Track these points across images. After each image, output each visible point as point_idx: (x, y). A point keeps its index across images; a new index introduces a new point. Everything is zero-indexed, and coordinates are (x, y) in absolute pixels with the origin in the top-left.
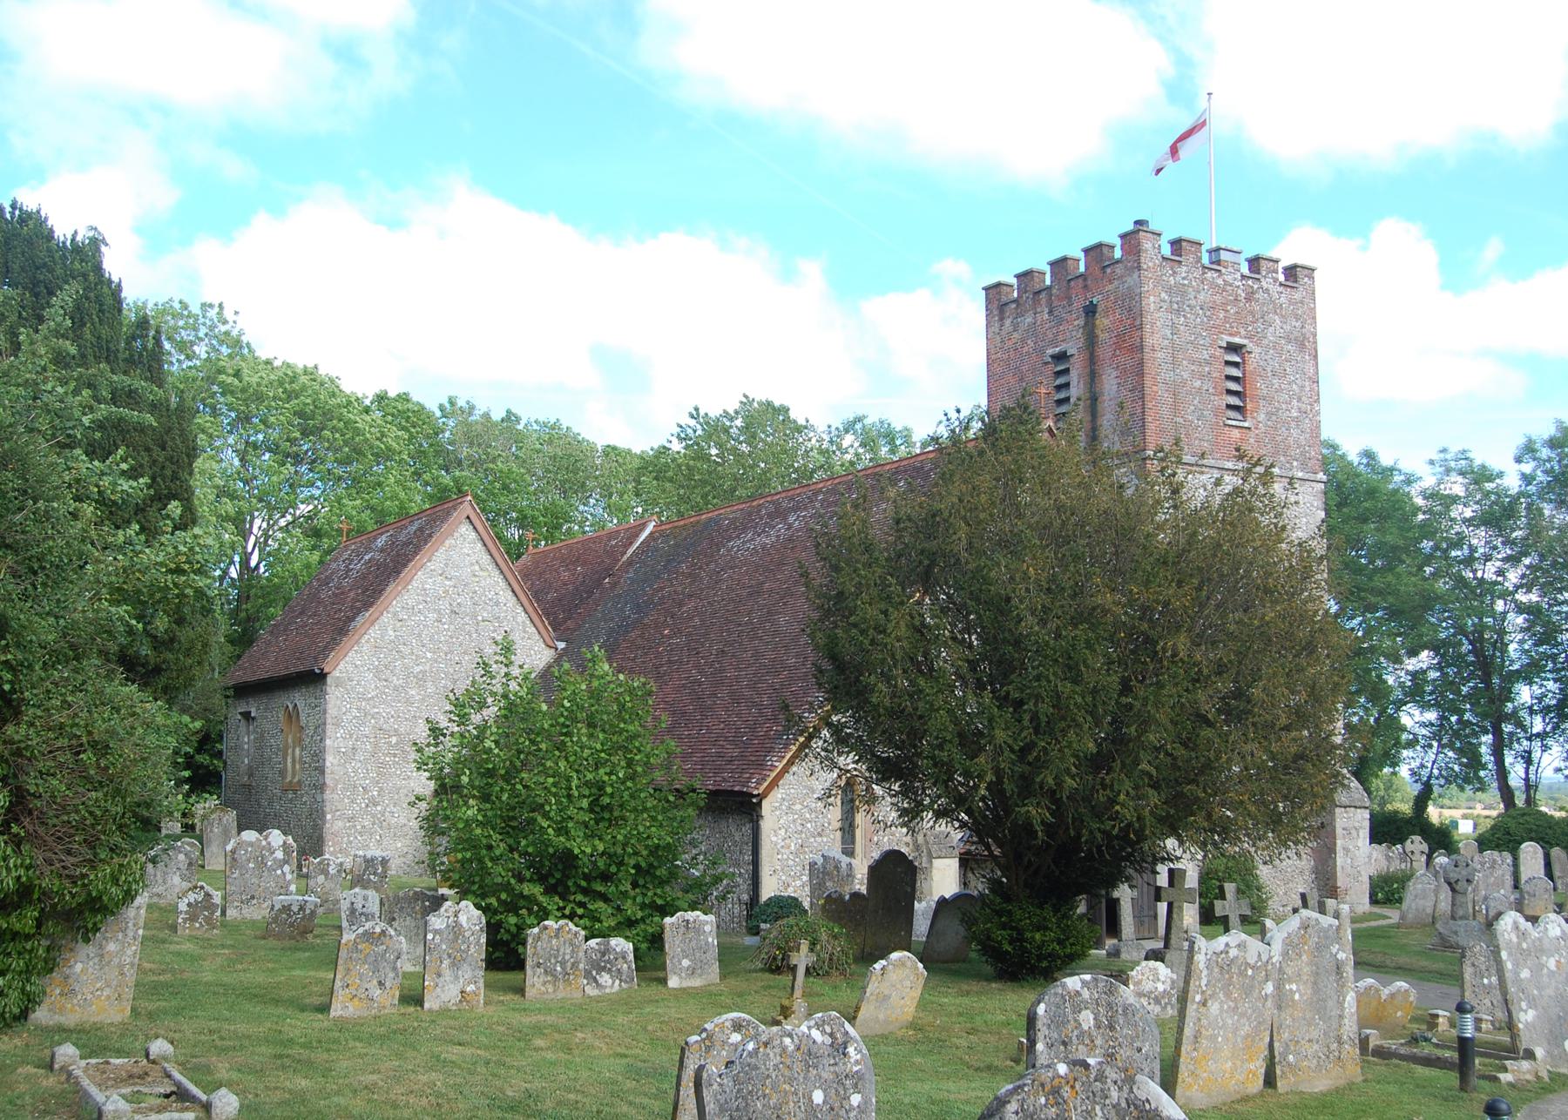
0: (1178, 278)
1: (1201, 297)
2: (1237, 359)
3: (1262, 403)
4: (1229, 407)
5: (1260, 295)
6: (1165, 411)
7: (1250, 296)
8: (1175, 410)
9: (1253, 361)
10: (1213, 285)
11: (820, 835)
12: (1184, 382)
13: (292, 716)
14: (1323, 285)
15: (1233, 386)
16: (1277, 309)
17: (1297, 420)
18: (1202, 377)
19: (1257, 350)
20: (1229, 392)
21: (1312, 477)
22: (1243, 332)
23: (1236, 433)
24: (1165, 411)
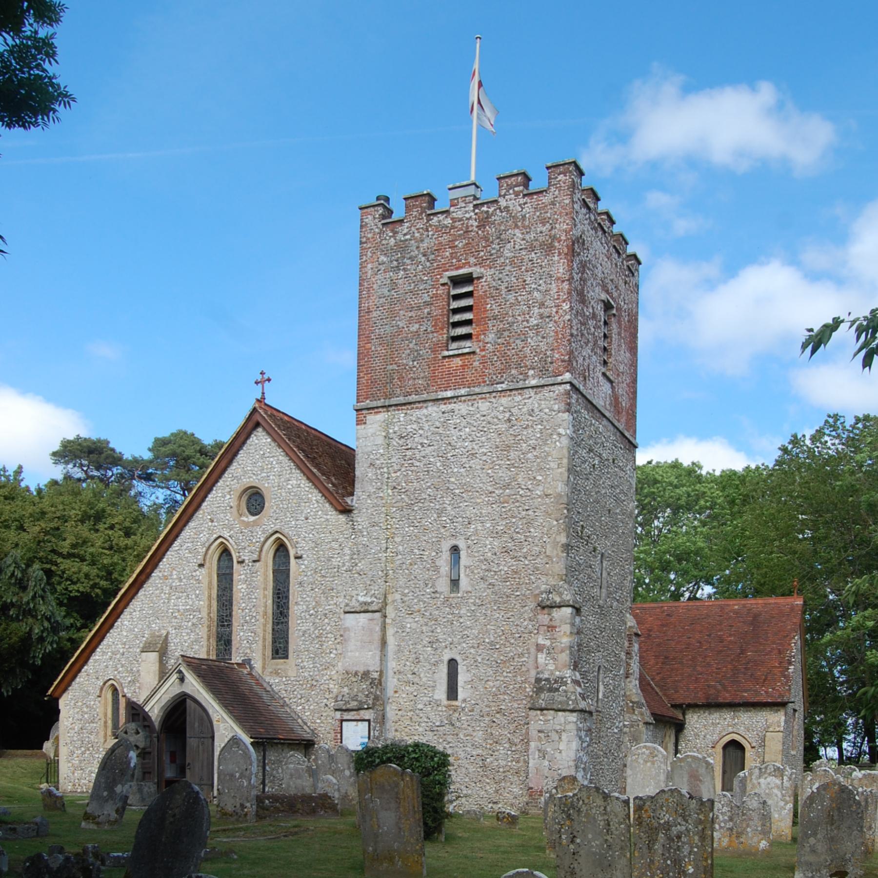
0: (400, 237)
1: (425, 245)
2: (470, 289)
3: (490, 324)
5: (498, 217)
7: (484, 222)
9: (480, 288)
10: (440, 228)
11: (92, 722)
12: (400, 330)
16: (517, 221)
18: (420, 320)
19: (488, 273)
21: (551, 381)
22: (472, 260)
23: (458, 361)
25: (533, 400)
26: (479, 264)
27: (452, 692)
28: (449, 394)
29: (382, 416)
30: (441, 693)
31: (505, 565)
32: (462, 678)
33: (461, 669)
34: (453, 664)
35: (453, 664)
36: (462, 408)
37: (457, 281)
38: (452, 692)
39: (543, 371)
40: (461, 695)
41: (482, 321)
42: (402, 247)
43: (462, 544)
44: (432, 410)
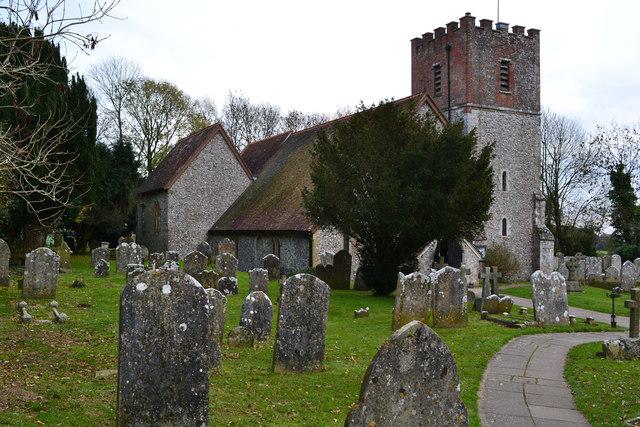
4: (502, 86)
6: (475, 88)
7: (512, 41)
8: (479, 88)
13: (157, 205)
14: (543, 37)
15: (504, 78)
17: (530, 91)
18: (491, 74)
20: (503, 80)
24: (475, 88)
25: (529, 119)
26: (514, 58)
27: (504, 233)
28: (501, 108)
29: (478, 111)
30: (501, 233)
31: (521, 182)
32: (508, 226)
33: (508, 222)
34: (504, 220)
35: (504, 220)
36: (507, 116)
37: (504, 63)
38: (504, 233)
39: (533, 109)
40: (508, 233)
41: (513, 82)
42: (484, 40)
43: (508, 171)
44: (496, 113)
